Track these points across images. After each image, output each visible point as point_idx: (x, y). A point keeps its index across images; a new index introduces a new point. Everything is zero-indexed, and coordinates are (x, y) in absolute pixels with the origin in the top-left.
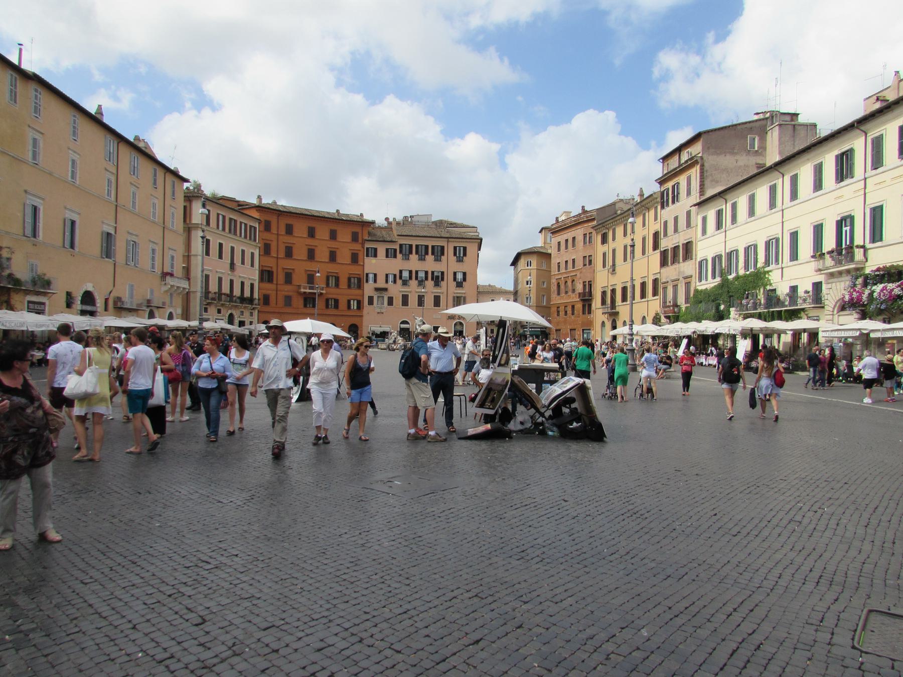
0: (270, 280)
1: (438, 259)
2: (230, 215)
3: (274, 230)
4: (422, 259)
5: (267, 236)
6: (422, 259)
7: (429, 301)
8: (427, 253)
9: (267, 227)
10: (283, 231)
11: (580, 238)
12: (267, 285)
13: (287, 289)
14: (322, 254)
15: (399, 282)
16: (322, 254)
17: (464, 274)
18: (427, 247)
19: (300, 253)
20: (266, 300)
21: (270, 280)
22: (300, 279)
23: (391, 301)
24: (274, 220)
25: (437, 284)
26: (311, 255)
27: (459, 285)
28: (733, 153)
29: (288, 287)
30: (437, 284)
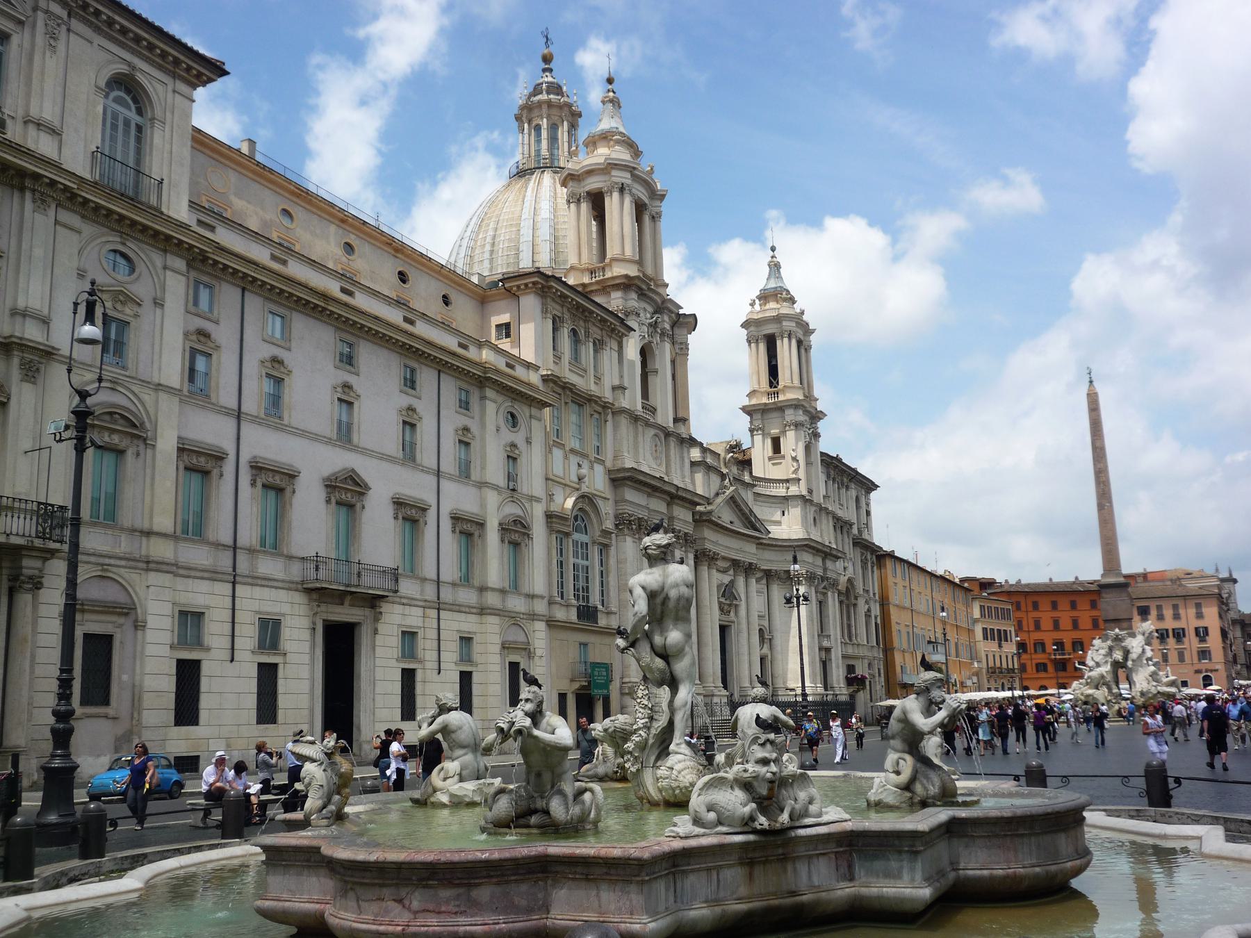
0: (1025, 651)
3: (1023, 608)
5: (1019, 614)
7: (1173, 657)
9: (1018, 607)
10: (1030, 608)
13: (1040, 658)
14: (1066, 623)
16: (1066, 623)
17: (1206, 628)
19: (1046, 624)
20: (1023, 668)
21: (1025, 651)
24: (1022, 600)
26: (1056, 626)
27: (1202, 640)
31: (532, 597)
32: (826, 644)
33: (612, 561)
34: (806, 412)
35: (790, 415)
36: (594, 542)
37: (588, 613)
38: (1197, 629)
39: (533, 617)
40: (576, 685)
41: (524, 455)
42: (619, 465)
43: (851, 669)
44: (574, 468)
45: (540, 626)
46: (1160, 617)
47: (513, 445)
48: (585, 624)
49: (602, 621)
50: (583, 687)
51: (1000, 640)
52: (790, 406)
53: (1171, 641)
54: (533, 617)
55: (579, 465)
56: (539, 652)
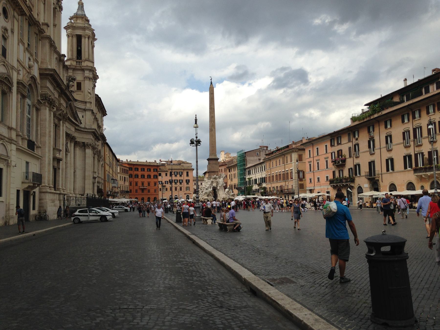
1: (181, 176)
2: (124, 168)
4: (176, 176)
6: (176, 176)
8: (177, 174)
11: (223, 170)
12: (130, 187)
13: (136, 188)
15: (169, 183)
18: (177, 172)
22: (140, 184)
23: (167, 189)
25: (181, 183)
28: (253, 156)
29: (137, 187)
30: (181, 183)
31: (10, 128)
32: (95, 176)
33: (39, 119)
34: (93, 74)
35: (87, 73)
36: (34, 106)
37: (31, 145)
38: (186, 180)
39: (11, 141)
40: (26, 185)
41: (10, 38)
42: (44, 66)
43: (98, 187)
44: (27, 60)
45: (14, 147)
46: (171, 175)
47: (6, 30)
48: (30, 151)
49: (35, 150)
50: (29, 186)
51: (125, 181)
52: (87, 69)
53: (178, 183)
54: (11, 141)
55: (29, 59)
56: (13, 164)
